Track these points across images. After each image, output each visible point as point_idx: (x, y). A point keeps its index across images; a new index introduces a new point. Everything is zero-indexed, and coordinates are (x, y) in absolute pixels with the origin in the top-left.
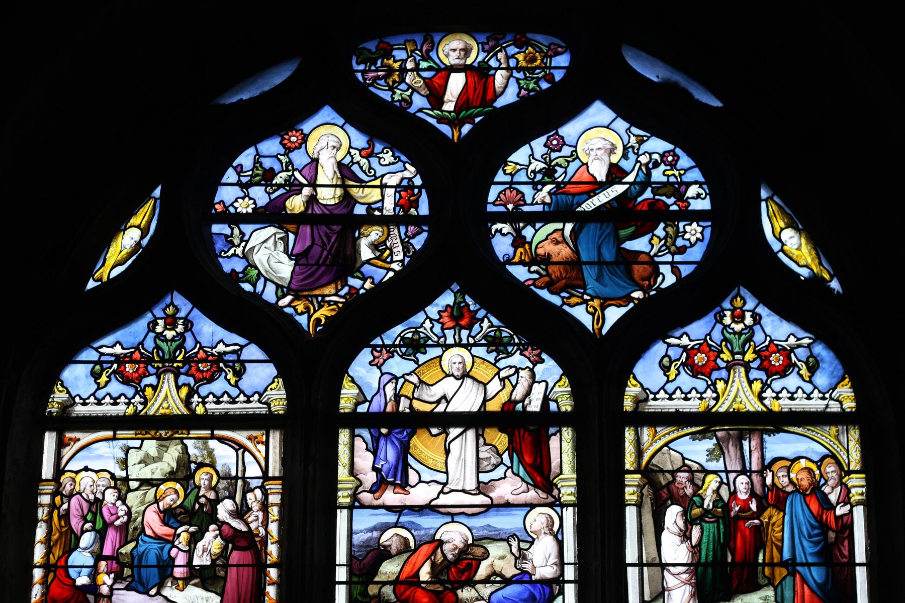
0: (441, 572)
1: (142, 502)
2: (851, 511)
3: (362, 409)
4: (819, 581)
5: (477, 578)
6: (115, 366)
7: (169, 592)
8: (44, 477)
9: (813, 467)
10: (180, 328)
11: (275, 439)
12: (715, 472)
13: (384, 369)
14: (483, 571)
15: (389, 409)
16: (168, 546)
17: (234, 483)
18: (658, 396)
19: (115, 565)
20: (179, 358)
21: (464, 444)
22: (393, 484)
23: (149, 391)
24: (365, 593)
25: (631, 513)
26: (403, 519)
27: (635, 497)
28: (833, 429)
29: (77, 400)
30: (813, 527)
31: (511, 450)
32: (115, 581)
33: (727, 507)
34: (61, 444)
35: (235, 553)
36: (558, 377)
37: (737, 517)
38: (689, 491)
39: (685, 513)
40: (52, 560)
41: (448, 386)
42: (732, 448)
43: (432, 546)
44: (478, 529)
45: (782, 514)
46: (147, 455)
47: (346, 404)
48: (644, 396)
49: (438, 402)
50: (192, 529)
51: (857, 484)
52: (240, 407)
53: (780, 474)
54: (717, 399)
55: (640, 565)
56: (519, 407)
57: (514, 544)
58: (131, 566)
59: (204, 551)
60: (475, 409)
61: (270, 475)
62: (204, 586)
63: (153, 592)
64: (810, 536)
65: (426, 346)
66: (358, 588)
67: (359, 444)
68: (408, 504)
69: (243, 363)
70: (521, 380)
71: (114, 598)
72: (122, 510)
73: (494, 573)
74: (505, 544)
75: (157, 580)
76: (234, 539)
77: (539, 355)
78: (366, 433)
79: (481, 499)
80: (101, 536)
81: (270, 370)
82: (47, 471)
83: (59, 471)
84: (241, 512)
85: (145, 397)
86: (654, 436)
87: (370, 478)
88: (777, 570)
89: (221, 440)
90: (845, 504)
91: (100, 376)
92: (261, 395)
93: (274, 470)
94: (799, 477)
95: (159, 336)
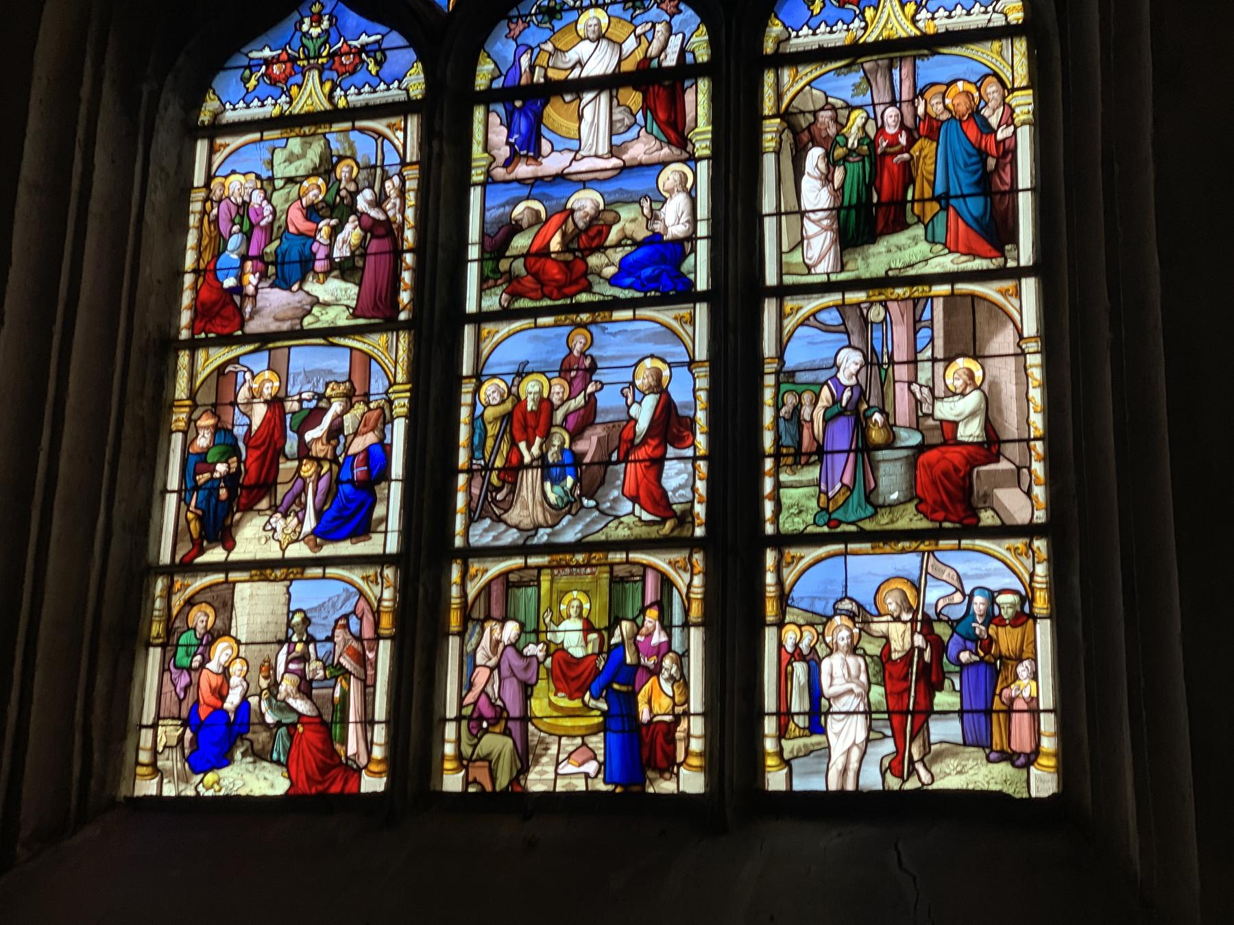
0: (572, 241)
1: (287, 200)
2: (1015, 133)
3: (498, 84)
4: (976, 214)
5: (608, 243)
6: (264, 68)
7: (312, 287)
8: (196, 185)
9: (972, 89)
10: (325, 24)
11: (413, 123)
12: (860, 107)
13: (519, 42)
14: (613, 236)
15: (523, 81)
16: (310, 241)
17: (374, 172)
18: (801, 33)
19: (260, 265)
20: (324, 54)
21: (596, 108)
22: (526, 156)
23: (294, 90)
24: (496, 270)
25: (769, 162)
26: (534, 192)
27: (773, 144)
28: (996, 45)
29: (228, 106)
30: (970, 155)
31: (645, 108)
32: (260, 280)
33: (873, 144)
34: (212, 151)
35: (375, 243)
36: (694, 27)
37: (884, 153)
38: (832, 131)
39: (827, 155)
40: (202, 266)
41: (585, 49)
42: (880, 79)
43: (564, 215)
44: (609, 194)
45: (935, 144)
46: (292, 153)
47: (481, 83)
48: (786, 35)
49: (573, 68)
50: (333, 222)
51: (1023, 103)
52: (383, 95)
53: (934, 102)
54: (865, 28)
55: (778, 214)
56: (655, 63)
57: (646, 204)
58: (274, 263)
59: (344, 242)
60: (610, 71)
61: (408, 160)
62: (343, 277)
63: (295, 287)
64: (966, 165)
65: (562, 10)
66: (489, 265)
67: (494, 119)
68: (540, 174)
69: (383, 51)
70: (658, 35)
71: (259, 297)
72: (267, 209)
73: (626, 237)
74: (637, 206)
75: (299, 276)
76: (372, 228)
77: (677, 6)
78: (500, 108)
79: (614, 162)
80: (248, 237)
81: (411, 55)
82: (199, 179)
83: (210, 177)
84: (379, 202)
85: (290, 97)
86: (795, 76)
87: (505, 152)
88: (928, 205)
89: (362, 131)
90: (1008, 126)
91: (249, 79)
92: (400, 82)
93: (412, 154)
94: (956, 102)
95: (305, 34)
